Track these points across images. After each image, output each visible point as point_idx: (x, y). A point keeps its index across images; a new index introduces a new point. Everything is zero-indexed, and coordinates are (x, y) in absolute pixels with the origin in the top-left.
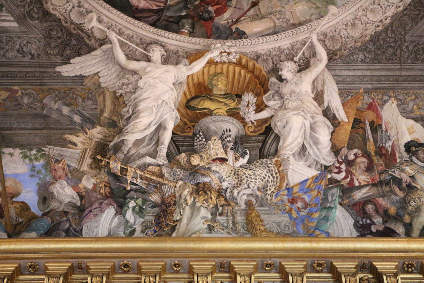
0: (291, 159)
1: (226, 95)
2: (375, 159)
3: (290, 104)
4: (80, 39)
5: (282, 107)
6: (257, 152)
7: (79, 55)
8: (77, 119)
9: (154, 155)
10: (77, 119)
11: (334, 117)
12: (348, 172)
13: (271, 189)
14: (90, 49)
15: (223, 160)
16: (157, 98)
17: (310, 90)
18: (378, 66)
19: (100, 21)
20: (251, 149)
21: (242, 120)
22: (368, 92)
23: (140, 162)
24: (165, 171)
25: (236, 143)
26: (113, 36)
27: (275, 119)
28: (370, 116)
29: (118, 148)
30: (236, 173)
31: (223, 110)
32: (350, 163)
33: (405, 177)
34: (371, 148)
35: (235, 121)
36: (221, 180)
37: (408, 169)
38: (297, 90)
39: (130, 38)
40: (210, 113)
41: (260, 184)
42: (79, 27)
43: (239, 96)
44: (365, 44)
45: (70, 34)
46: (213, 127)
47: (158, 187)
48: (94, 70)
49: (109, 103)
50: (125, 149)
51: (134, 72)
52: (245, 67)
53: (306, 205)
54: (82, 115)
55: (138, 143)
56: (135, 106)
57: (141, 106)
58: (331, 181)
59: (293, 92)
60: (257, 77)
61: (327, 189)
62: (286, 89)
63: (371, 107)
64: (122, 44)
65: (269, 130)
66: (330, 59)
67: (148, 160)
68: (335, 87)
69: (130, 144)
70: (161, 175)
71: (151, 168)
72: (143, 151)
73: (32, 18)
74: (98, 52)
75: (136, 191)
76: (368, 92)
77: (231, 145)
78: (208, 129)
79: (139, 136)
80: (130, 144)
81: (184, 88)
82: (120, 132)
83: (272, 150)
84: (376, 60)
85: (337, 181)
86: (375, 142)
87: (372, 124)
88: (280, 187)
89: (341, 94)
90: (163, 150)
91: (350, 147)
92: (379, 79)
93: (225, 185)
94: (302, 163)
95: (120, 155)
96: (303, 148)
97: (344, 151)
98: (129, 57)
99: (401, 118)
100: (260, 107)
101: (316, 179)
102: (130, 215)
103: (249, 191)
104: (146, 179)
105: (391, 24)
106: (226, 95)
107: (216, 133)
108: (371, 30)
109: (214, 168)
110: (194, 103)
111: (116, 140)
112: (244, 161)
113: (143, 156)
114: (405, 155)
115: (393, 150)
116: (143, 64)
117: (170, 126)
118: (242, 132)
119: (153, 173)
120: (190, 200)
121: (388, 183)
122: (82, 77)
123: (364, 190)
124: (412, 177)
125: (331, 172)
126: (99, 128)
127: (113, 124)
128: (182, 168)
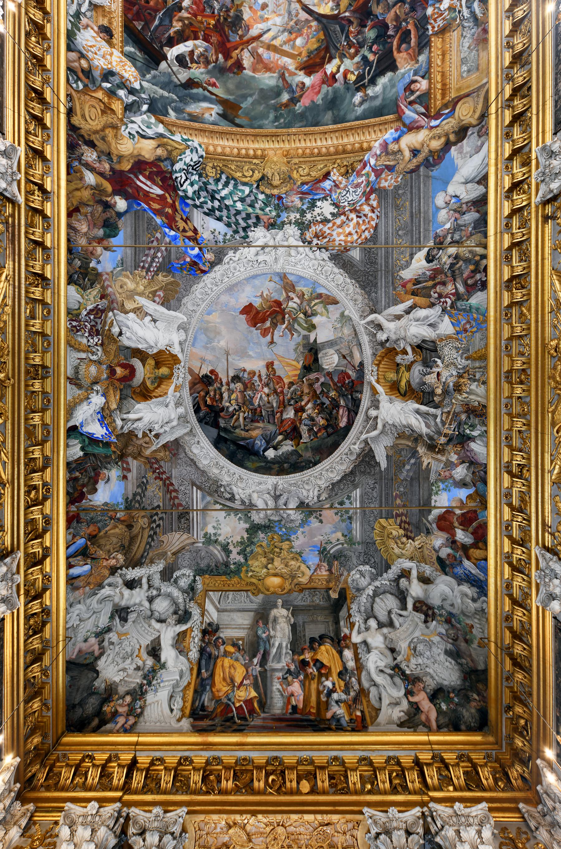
0: (437, 332)
1: (397, 372)
2: (437, 281)
3: (403, 334)
4: (366, 456)
5: (404, 339)
6: (433, 354)
7: (374, 457)
8: (413, 461)
9: (435, 417)
10: (413, 461)
11: (411, 307)
12: (446, 297)
13: (458, 344)
14: (371, 450)
15: (439, 374)
16: (400, 414)
17: (394, 323)
18: (379, 284)
19: (355, 444)
20: (431, 357)
21: (412, 363)
22: (394, 289)
23: (440, 425)
24: (446, 410)
25: (427, 366)
26: (363, 437)
27: (412, 343)
28: (410, 286)
29: (431, 438)
30: (447, 366)
31: (406, 374)
32: (440, 296)
33: (450, 261)
34: (430, 283)
35: (413, 367)
36: (452, 375)
37: (444, 260)
38: (393, 330)
39: (364, 427)
40: (408, 382)
41: (454, 351)
42: (358, 455)
43: (398, 365)
44: (366, 293)
45: (362, 461)
46: (417, 380)
47: (456, 415)
48: (383, 449)
49: (403, 442)
50: (432, 434)
51: (384, 426)
52: (380, 362)
53: (468, 322)
54: (410, 458)
55: (427, 426)
56: (405, 426)
57: (404, 423)
58: (452, 307)
59: (395, 333)
60: (386, 354)
61: (458, 309)
62: (393, 337)
63: (404, 286)
64: (368, 432)
65: (419, 347)
66: (375, 312)
67: (438, 420)
68: (392, 308)
69: (429, 431)
70: (449, 412)
71: (444, 419)
72: (433, 423)
73: (354, 480)
74: (373, 446)
75: (459, 429)
76: (394, 289)
77: (428, 370)
78: (418, 383)
79: (423, 425)
80: (428, 431)
81: (393, 397)
82: (421, 436)
83: (432, 344)
84: (375, 285)
85: (452, 303)
86: (426, 281)
87: (414, 285)
88: (456, 339)
89: (396, 304)
90: (432, 411)
91: (430, 296)
92: (387, 283)
93: (455, 373)
94: (440, 326)
95: (436, 437)
96: (430, 325)
97: (432, 300)
98: (375, 428)
100: (405, 352)
101: (450, 316)
102: (475, 433)
103: (459, 359)
104: (451, 421)
105: (355, 279)
106: (397, 372)
107: (421, 379)
108: (358, 290)
109: (444, 380)
110: (402, 391)
111: (426, 439)
112: (439, 362)
113: (436, 423)
114: (434, 263)
115: (432, 270)
116: (379, 421)
117: (417, 406)
118: (421, 363)
119: (447, 417)
120: (465, 395)
121: (453, 272)
122: (387, 456)
124: (449, 257)
125: (446, 308)
126: (419, 449)
127: (416, 440)
128: (444, 400)
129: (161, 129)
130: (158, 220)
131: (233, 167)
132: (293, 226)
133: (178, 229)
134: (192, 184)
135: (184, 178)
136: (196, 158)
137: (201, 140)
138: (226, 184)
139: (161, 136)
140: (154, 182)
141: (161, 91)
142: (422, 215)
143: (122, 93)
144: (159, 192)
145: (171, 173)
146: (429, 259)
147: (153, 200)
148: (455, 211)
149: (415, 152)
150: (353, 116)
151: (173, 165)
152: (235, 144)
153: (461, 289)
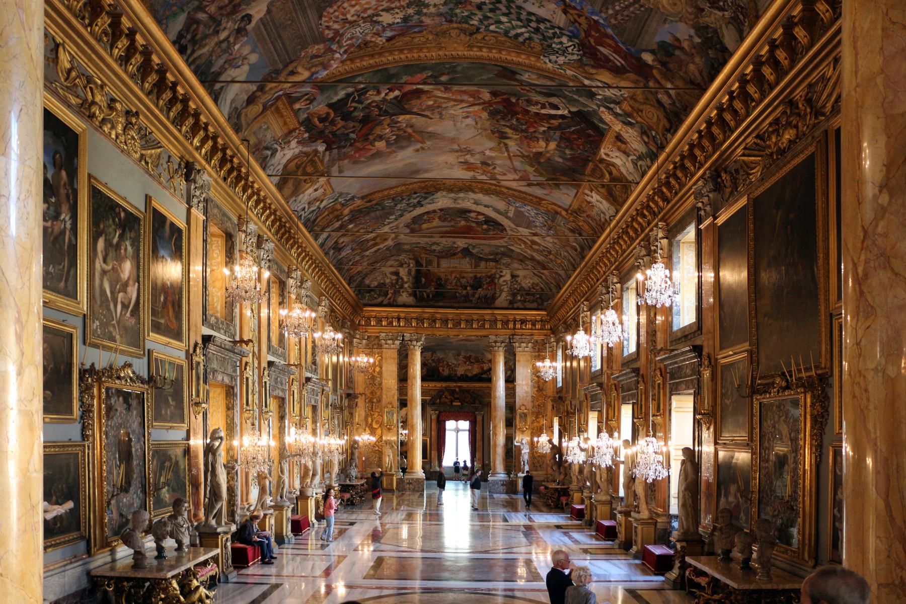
99: (266, 4)
123: (205, 15)
129: (587, 82)
130: (609, 31)
131: (508, 44)
132: (432, 3)
133: (586, 18)
134: (561, 43)
135: (570, 49)
136: (553, 58)
137: (544, 66)
138: (517, 36)
139: (587, 79)
140: (605, 56)
141: (580, 99)
142: (269, 42)
143: (618, 111)
144: (601, 49)
145: (584, 55)
146: (249, 18)
147: (610, 46)
148: (235, 59)
149: (292, 73)
150: (366, 76)
151: (580, 60)
152: (503, 57)
153: (201, 16)
